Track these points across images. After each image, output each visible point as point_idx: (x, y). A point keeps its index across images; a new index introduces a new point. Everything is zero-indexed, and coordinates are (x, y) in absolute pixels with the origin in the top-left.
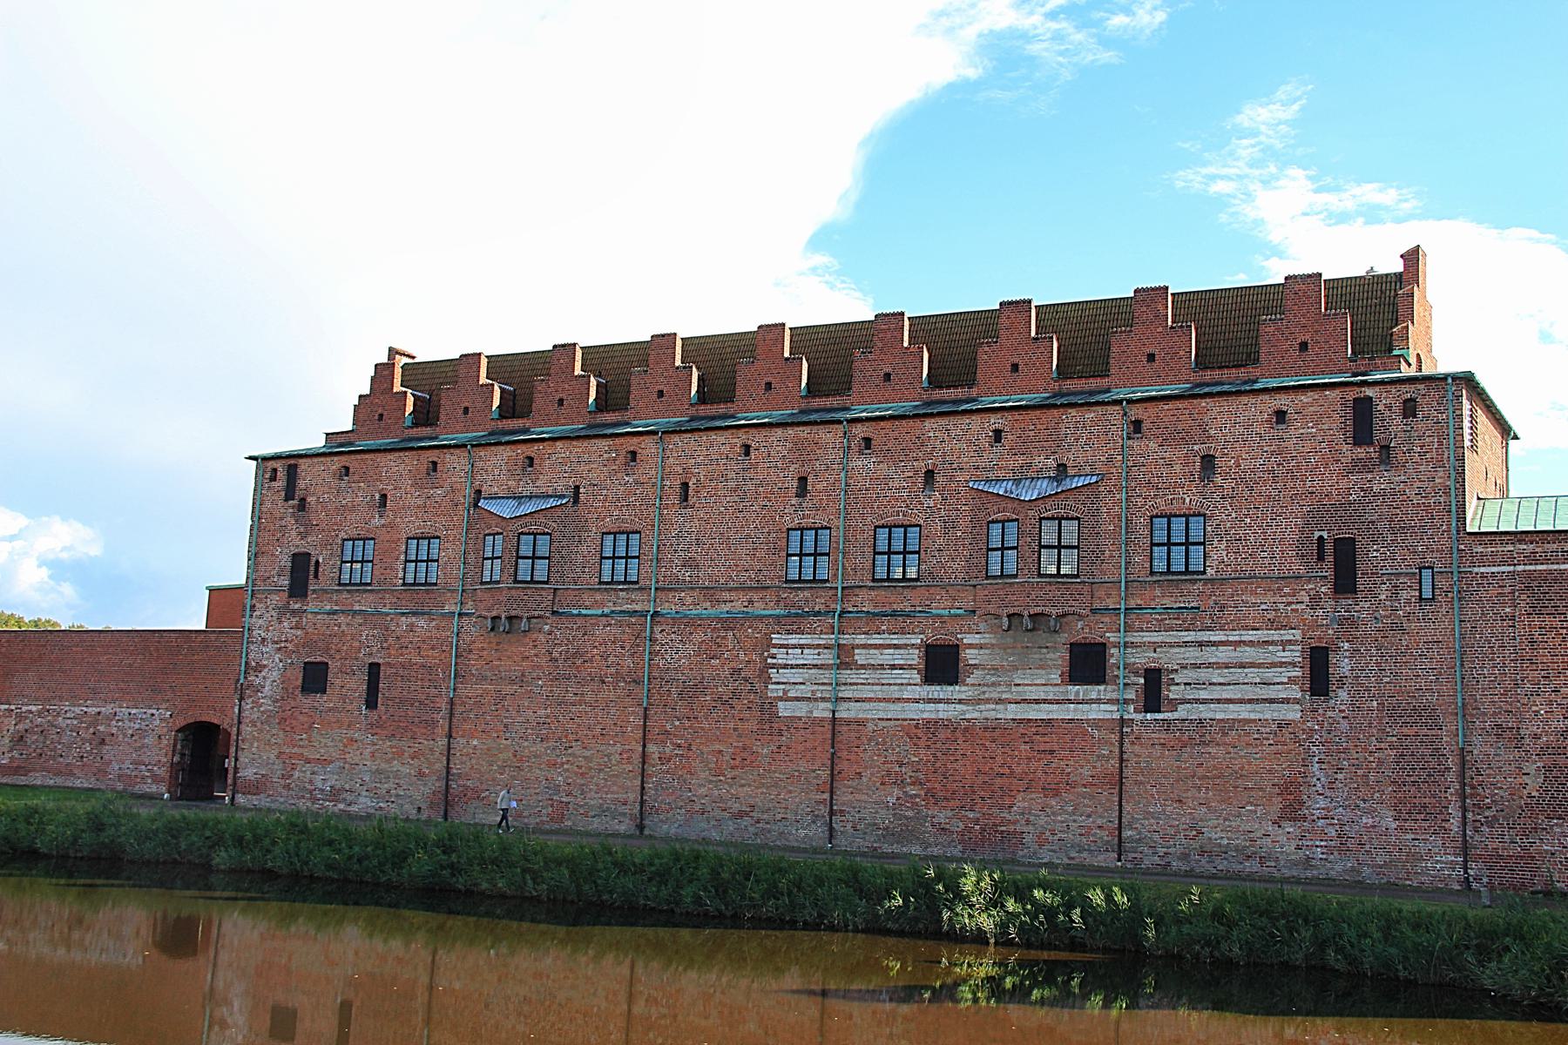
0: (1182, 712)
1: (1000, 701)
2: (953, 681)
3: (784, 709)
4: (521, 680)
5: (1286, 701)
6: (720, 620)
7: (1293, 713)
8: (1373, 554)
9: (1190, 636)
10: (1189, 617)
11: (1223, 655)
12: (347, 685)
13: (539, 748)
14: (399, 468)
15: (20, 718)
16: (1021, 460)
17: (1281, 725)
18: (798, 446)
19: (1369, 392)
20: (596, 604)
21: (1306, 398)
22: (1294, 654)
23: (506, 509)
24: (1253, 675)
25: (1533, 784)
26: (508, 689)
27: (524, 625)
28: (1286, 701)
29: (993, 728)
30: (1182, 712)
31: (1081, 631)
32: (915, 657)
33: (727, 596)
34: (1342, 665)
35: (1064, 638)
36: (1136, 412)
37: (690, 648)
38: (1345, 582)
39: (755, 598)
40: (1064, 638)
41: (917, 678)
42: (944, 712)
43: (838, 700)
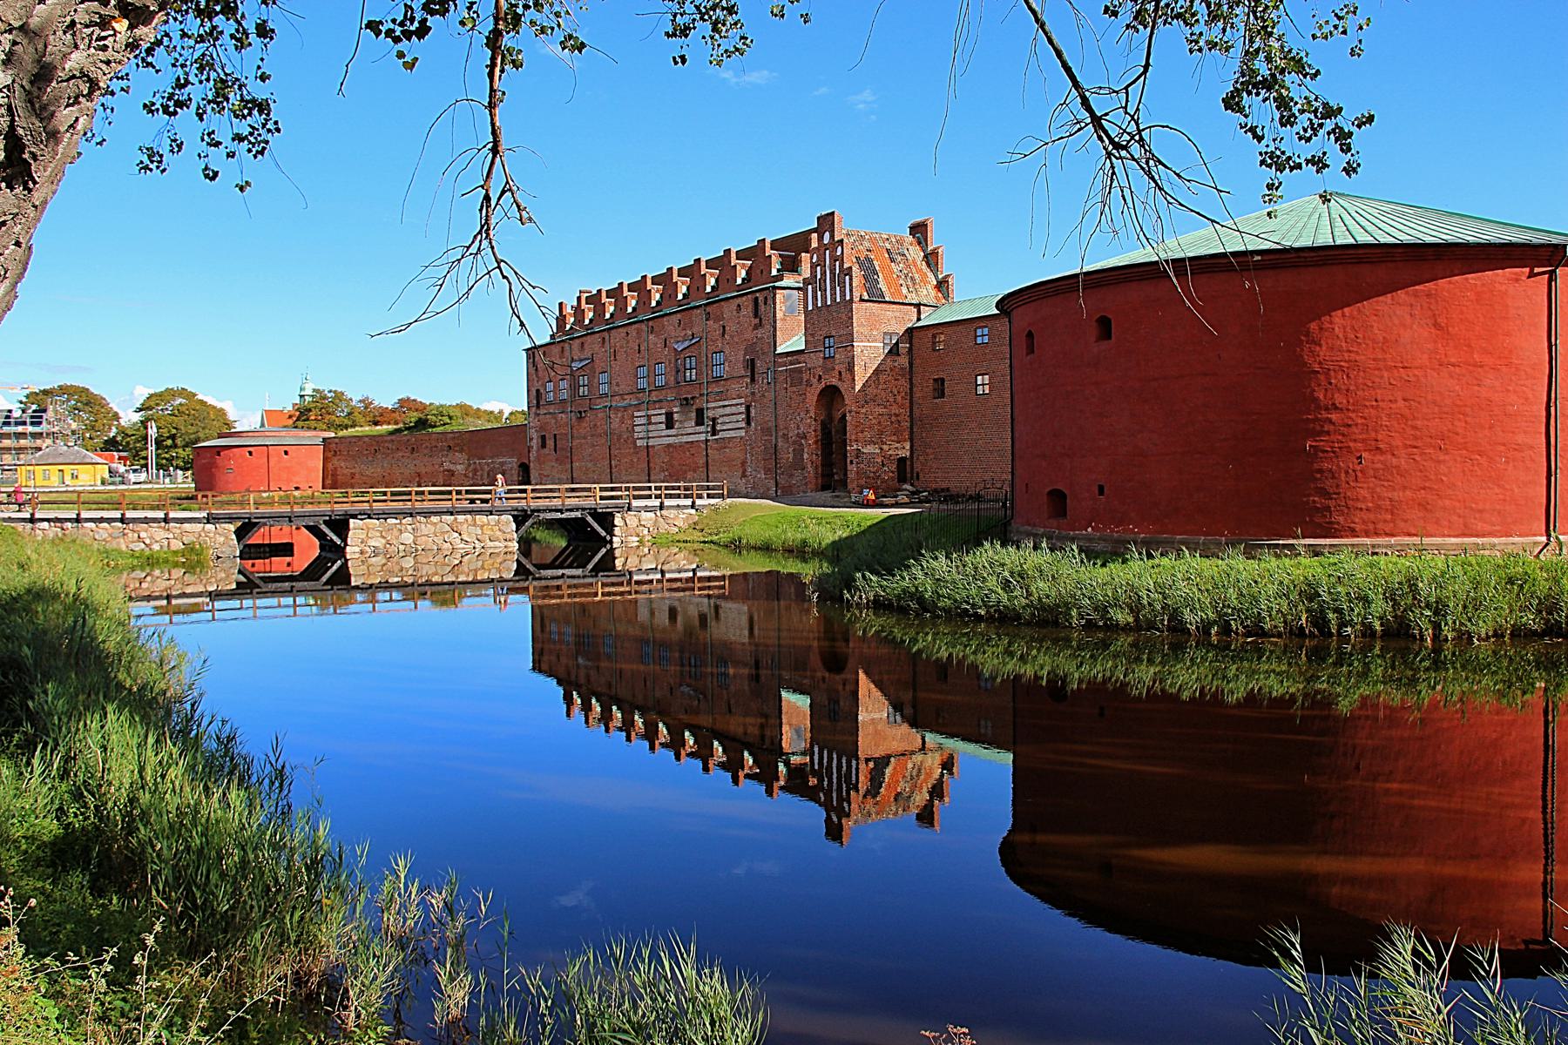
0: (721, 435)
1: (682, 435)
2: (672, 428)
3: (639, 443)
4: (585, 438)
5: (741, 428)
6: (624, 407)
7: (742, 433)
8: (758, 363)
9: (721, 403)
10: (722, 396)
11: (728, 410)
12: (550, 443)
13: (590, 465)
14: (556, 350)
15: (488, 464)
16: (684, 332)
17: (741, 438)
18: (639, 332)
19: (758, 295)
20: (600, 404)
21: (744, 299)
22: (743, 409)
23: (576, 365)
24: (734, 418)
25: (791, 456)
26: (583, 441)
27: (583, 415)
28: (741, 428)
29: (681, 445)
30: (721, 435)
31: (698, 404)
32: (663, 418)
33: (626, 397)
34: (753, 411)
35: (694, 407)
36: (708, 309)
37: (617, 420)
38: (753, 380)
39: (631, 396)
40: (694, 407)
41: (664, 426)
42: (671, 440)
43: (649, 438)
